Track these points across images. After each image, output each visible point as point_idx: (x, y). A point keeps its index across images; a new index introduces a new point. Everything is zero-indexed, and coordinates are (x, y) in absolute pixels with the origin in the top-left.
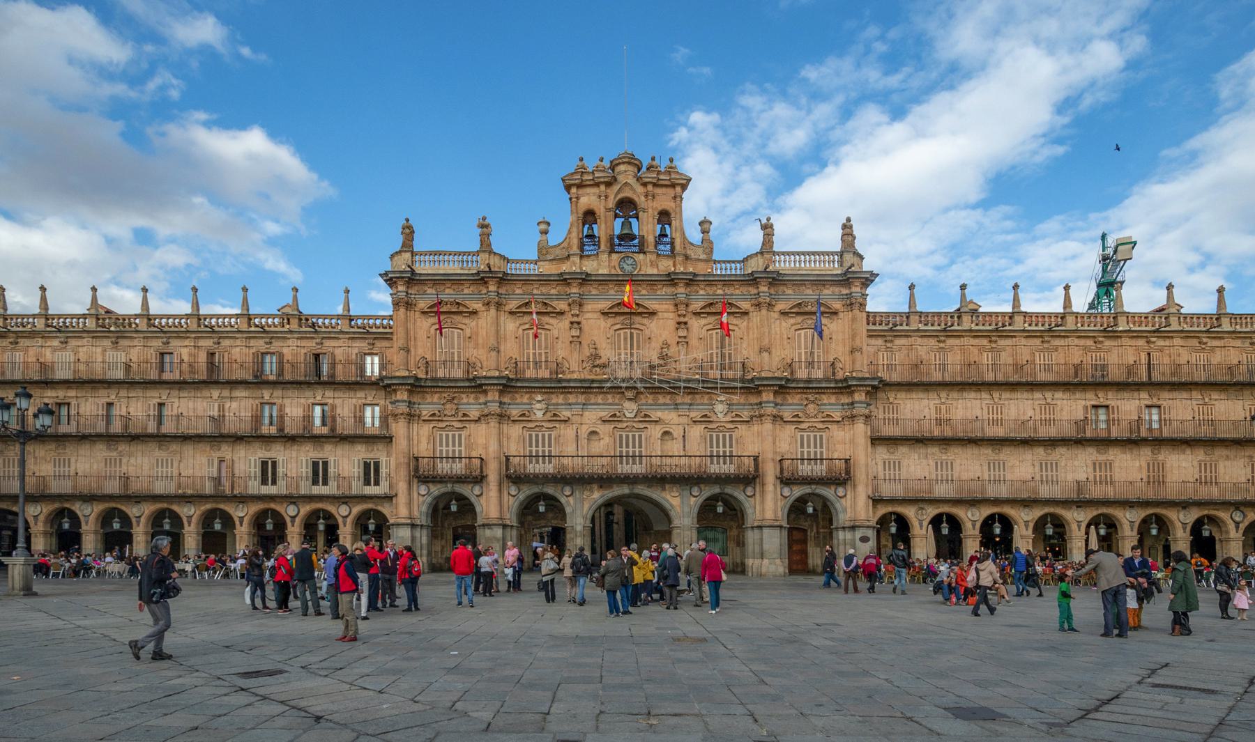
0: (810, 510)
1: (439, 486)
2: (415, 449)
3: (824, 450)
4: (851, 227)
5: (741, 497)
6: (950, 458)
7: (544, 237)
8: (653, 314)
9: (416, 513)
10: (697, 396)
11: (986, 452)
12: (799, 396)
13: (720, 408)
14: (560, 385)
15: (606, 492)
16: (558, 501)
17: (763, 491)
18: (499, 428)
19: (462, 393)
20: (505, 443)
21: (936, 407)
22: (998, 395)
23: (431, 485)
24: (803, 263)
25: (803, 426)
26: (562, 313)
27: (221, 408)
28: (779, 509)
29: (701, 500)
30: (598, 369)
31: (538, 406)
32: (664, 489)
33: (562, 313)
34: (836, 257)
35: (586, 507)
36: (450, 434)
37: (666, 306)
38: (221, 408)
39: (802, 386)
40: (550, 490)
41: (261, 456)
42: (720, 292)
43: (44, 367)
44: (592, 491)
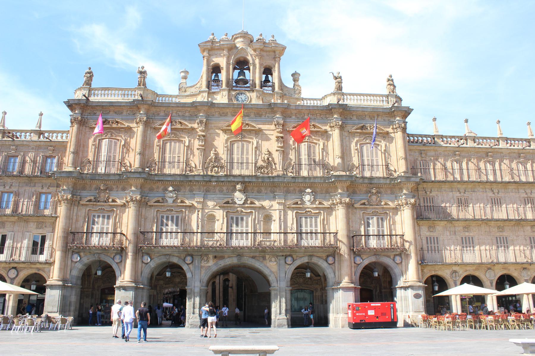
0: (376, 274)
2: (73, 226)
4: (392, 80)
6: (471, 234)
7: (184, 81)
11: (494, 230)
14: (187, 180)
16: (183, 269)
17: (340, 260)
18: (139, 211)
20: (143, 222)
21: (458, 199)
22: (497, 191)
28: (353, 274)
29: (293, 267)
30: (216, 169)
34: (384, 98)
35: (203, 271)
40: (175, 260)
44: (208, 261)
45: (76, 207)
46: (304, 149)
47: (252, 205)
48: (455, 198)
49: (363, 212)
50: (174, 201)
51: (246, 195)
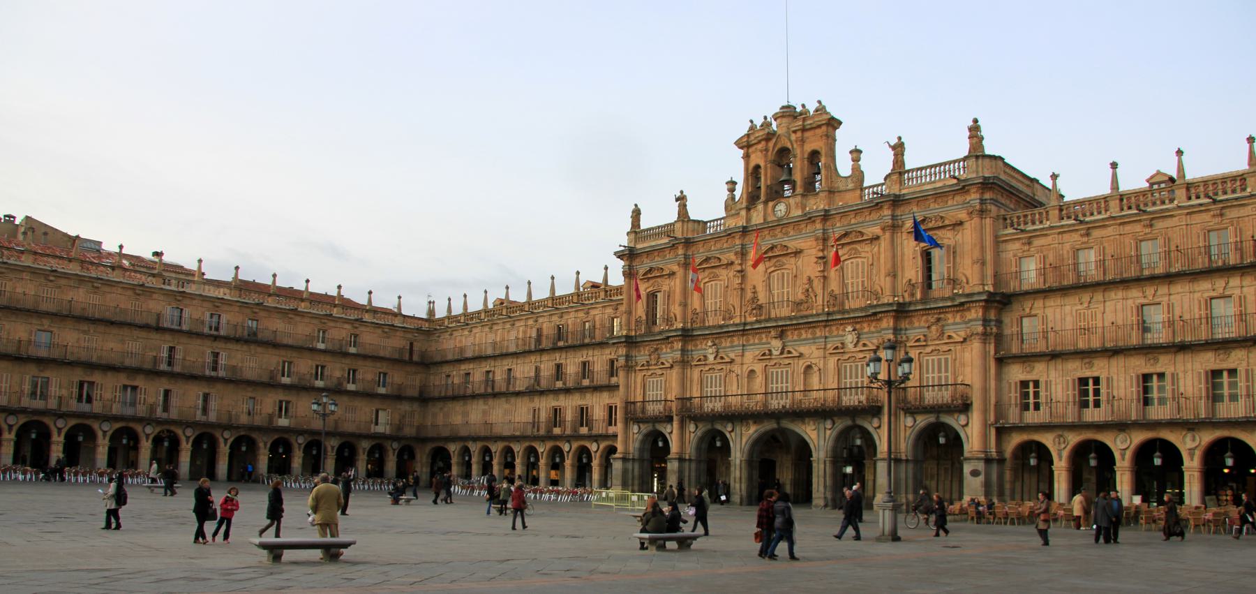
1: (646, 425)
3: (949, 374)
5: (871, 429)
8: (797, 253)
9: (631, 450)
10: (834, 328)
11: (1138, 363)
12: (924, 318)
13: (850, 339)
15: (758, 427)
19: (662, 344)
20: (688, 385)
23: (641, 425)
24: (928, 177)
25: (929, 349)
26: (732, 263)
27: (537, 370)
29: (835, 433)
31: (710, 351)
32: (804, 423)
33: (732, 263)
35: (744, 440)
36: (655, 380)
37: (809, 243)
38: (537, 370)
39: (920, 308)
41: (553, 404)
42: (853, 221)
43: (462, 350)
44: (748, 424)
45: (633, 374)
46: (852, 268)
47: (790, 355)
48: (1074, 314)
49: (920, 351)
50: (715, 358)
51: (783, 343)
